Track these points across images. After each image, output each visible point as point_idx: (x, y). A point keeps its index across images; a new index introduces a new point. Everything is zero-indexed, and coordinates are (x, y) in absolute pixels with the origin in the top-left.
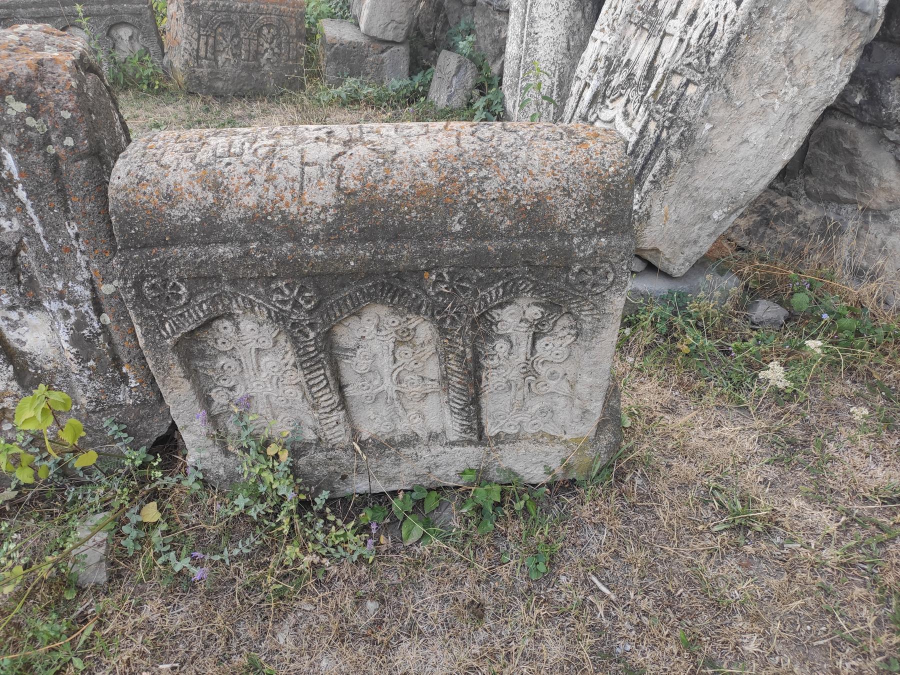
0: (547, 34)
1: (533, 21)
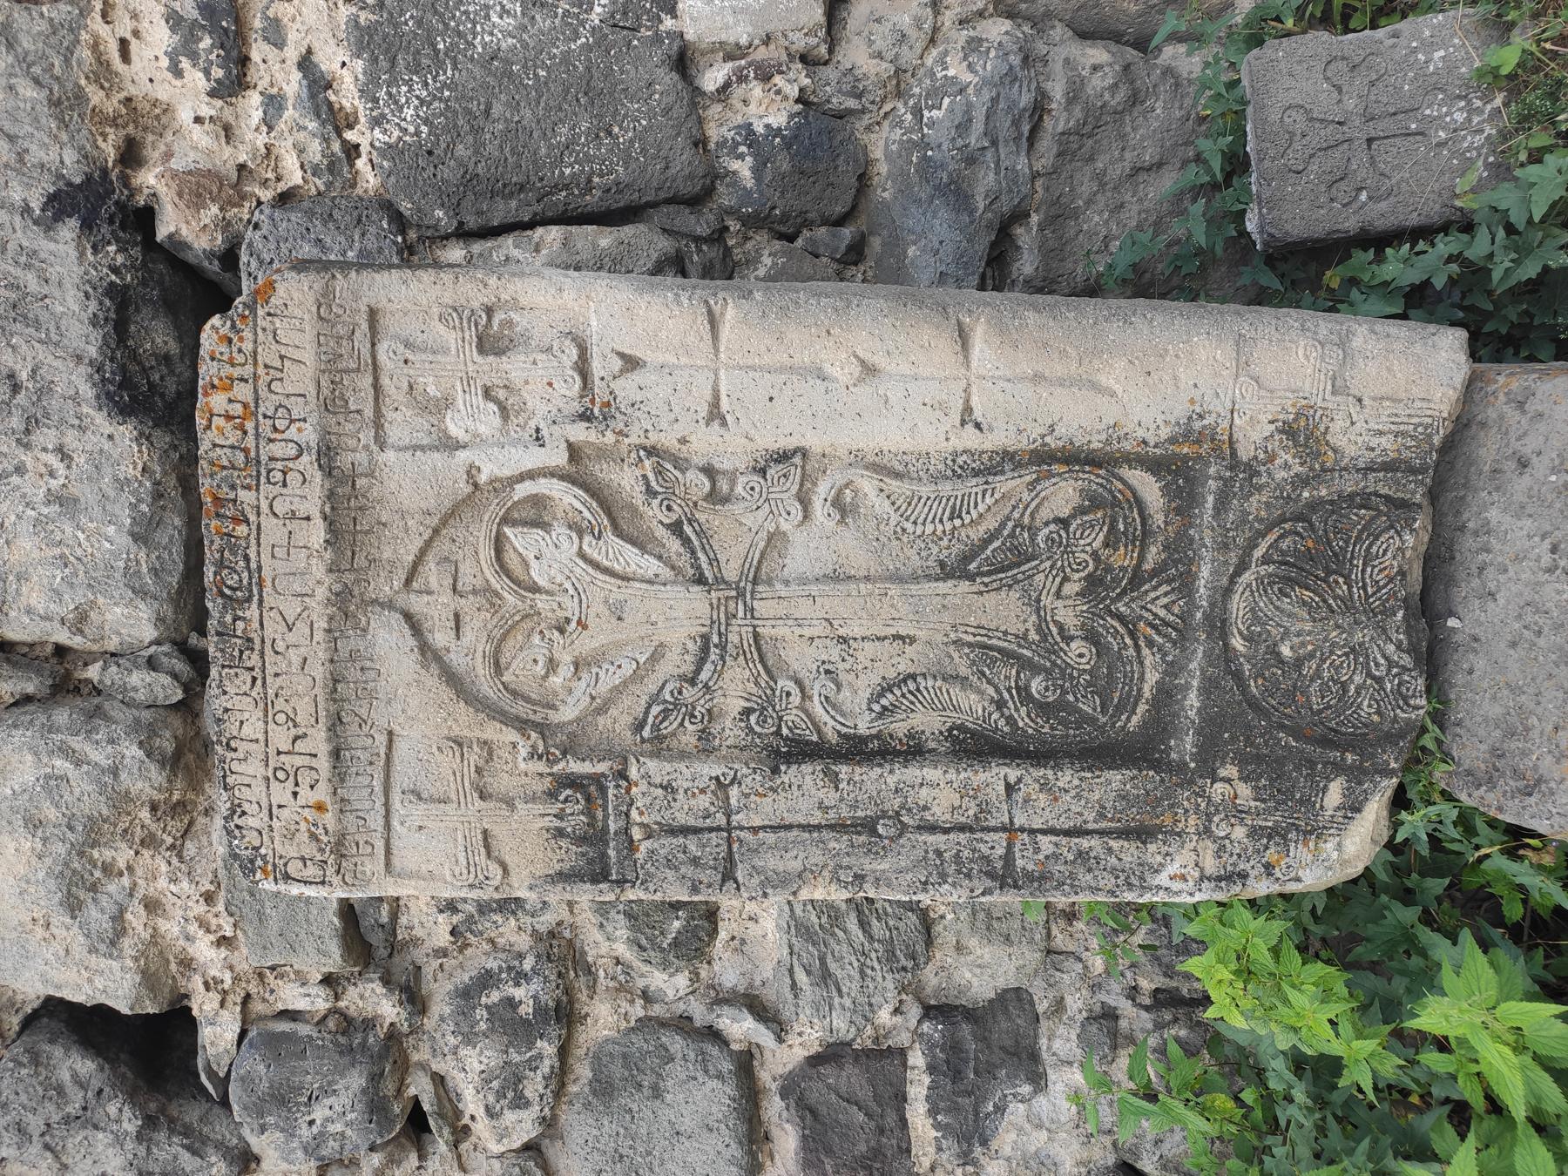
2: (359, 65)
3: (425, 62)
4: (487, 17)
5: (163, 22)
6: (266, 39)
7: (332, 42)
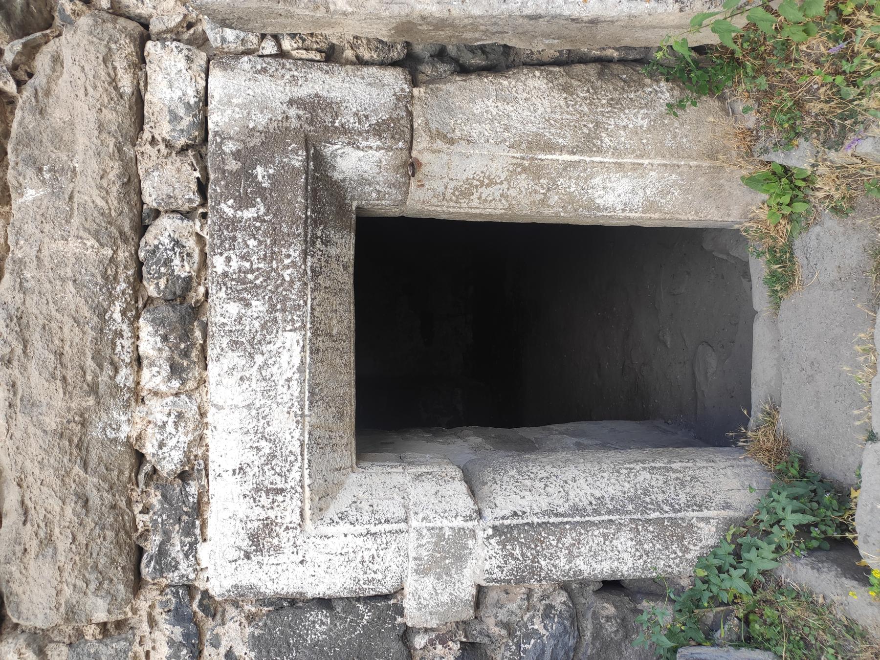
0: (585, 486)
1: (576, 510)
2: (253, 654)
3: (284, 650)
4: (314, 627)
5: (166, 644)
6: (211, 644)
7: (241, 644)
